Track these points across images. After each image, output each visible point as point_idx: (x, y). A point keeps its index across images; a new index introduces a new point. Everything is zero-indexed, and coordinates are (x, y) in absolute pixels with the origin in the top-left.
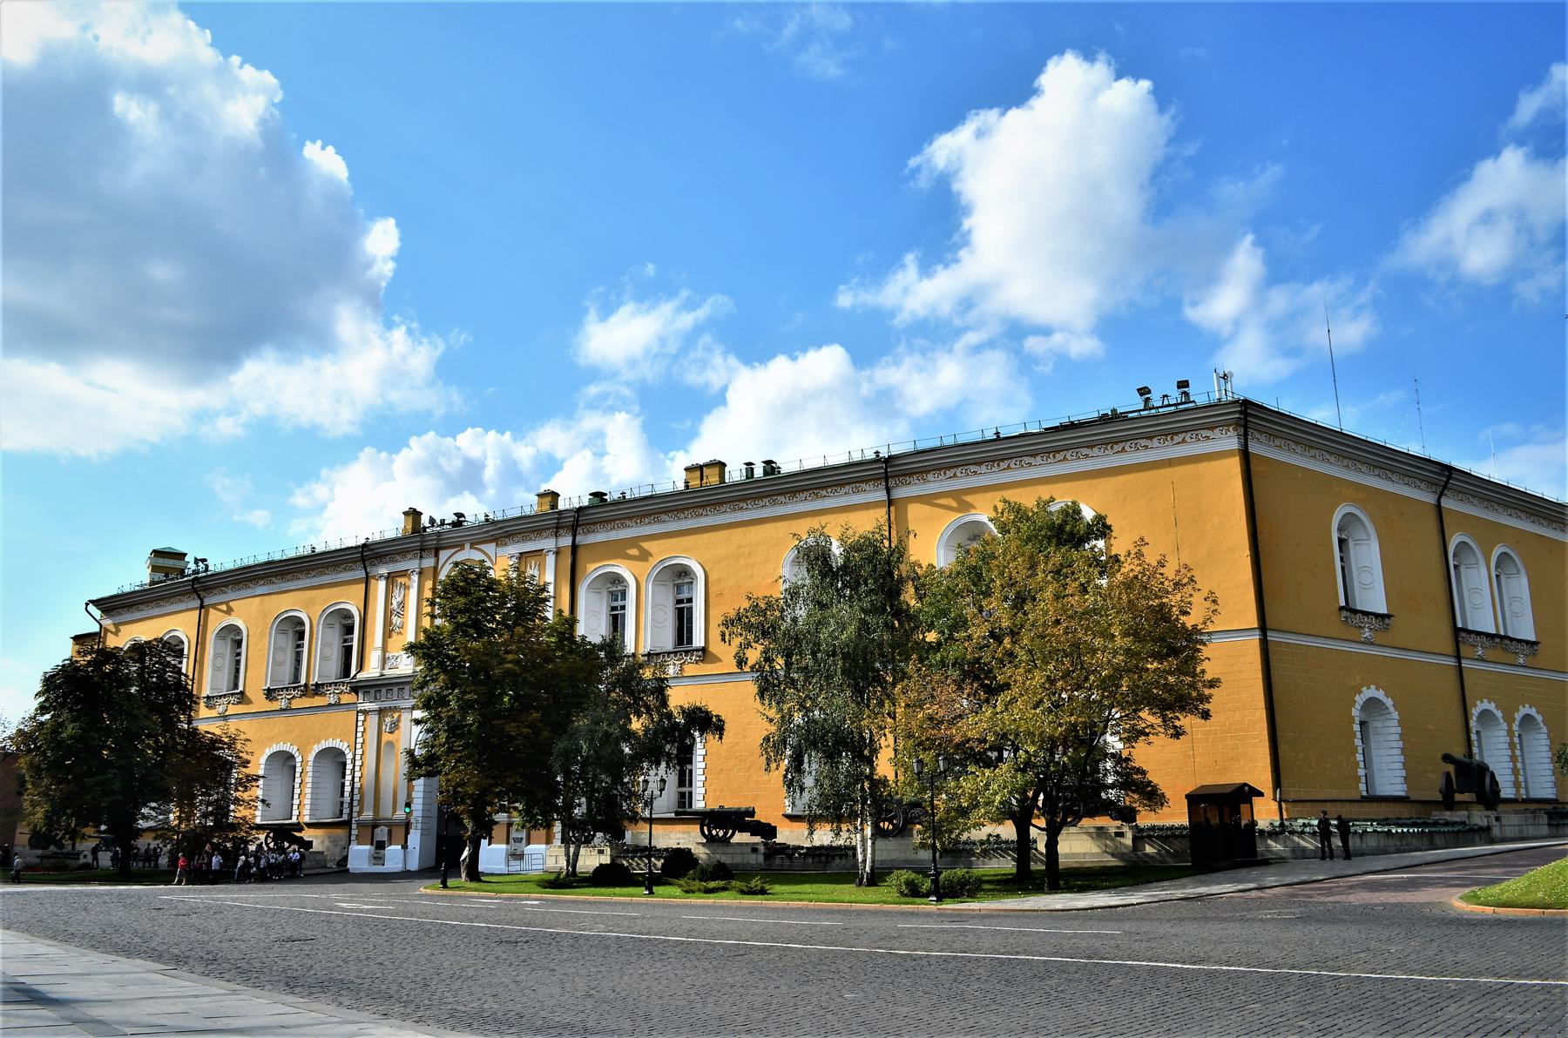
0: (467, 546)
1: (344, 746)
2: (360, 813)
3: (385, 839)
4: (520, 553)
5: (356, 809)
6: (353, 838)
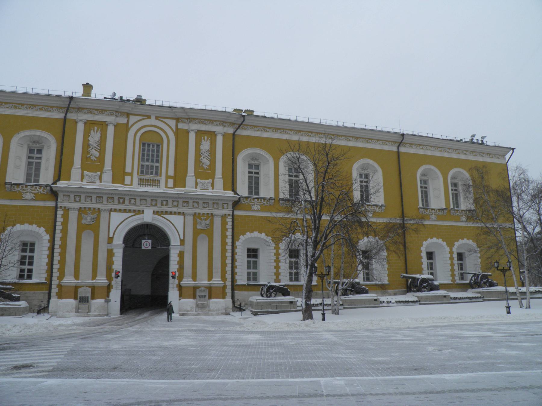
0: (153, 117)
2: (61, 277)
3: (89, 295)
4: (198, 130)
5: (56, 274)
6: (53, 294)
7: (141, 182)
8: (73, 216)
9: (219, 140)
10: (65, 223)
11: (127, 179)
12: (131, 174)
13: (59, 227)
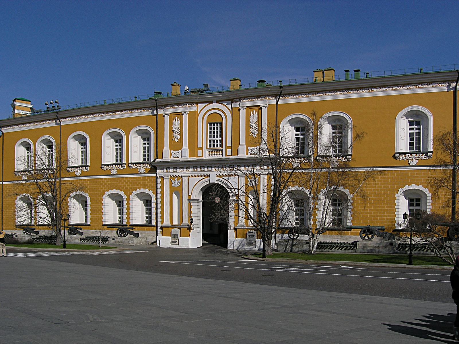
1: (150, 192)
7: (210, 153)
8: (167, 182)
9: (265, 111)
10: (162, 187)
11: (199, 153)
12: (201, 149)
13: (159, 190)
